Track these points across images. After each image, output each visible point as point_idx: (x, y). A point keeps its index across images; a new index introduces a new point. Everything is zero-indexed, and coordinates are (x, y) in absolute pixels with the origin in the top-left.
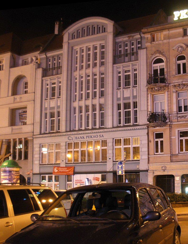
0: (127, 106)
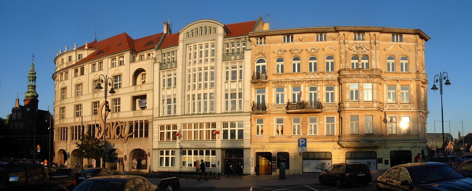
0: (233, 95)
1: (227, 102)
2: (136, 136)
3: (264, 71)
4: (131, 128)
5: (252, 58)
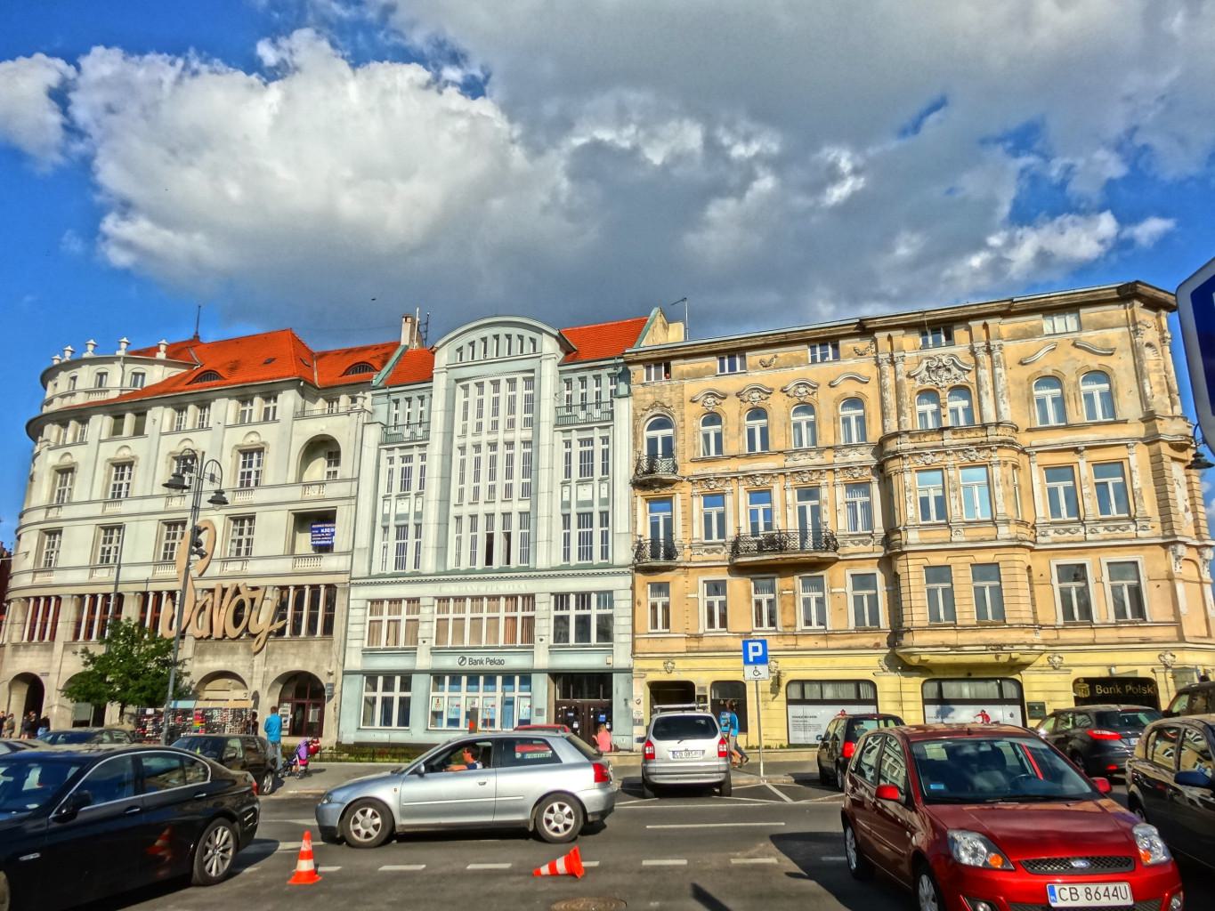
1: (567, 538)
2: (296, 630)
3: (669, 451)
4: (283, 605)
5: (636, 418)
